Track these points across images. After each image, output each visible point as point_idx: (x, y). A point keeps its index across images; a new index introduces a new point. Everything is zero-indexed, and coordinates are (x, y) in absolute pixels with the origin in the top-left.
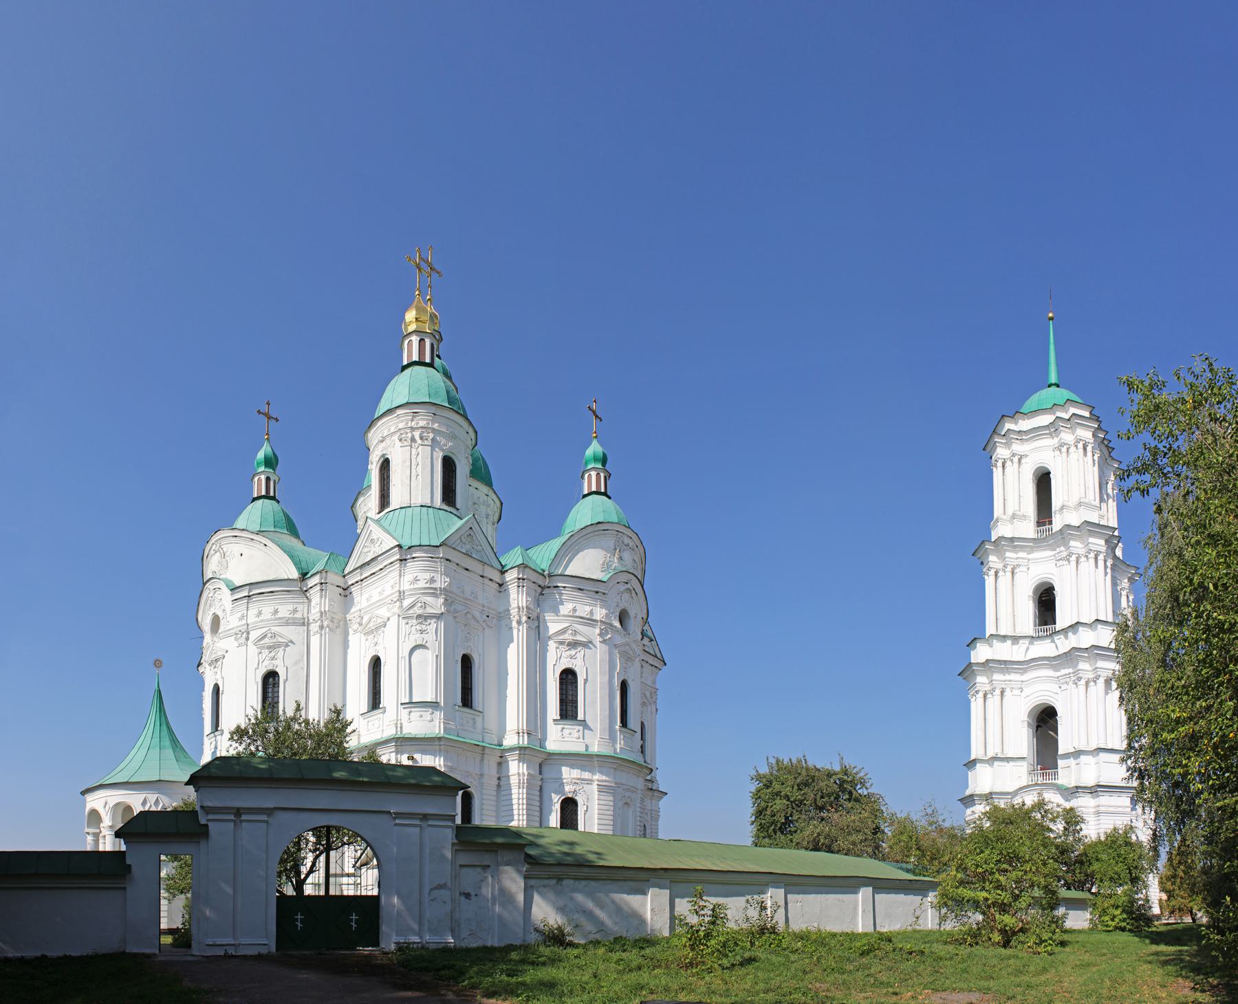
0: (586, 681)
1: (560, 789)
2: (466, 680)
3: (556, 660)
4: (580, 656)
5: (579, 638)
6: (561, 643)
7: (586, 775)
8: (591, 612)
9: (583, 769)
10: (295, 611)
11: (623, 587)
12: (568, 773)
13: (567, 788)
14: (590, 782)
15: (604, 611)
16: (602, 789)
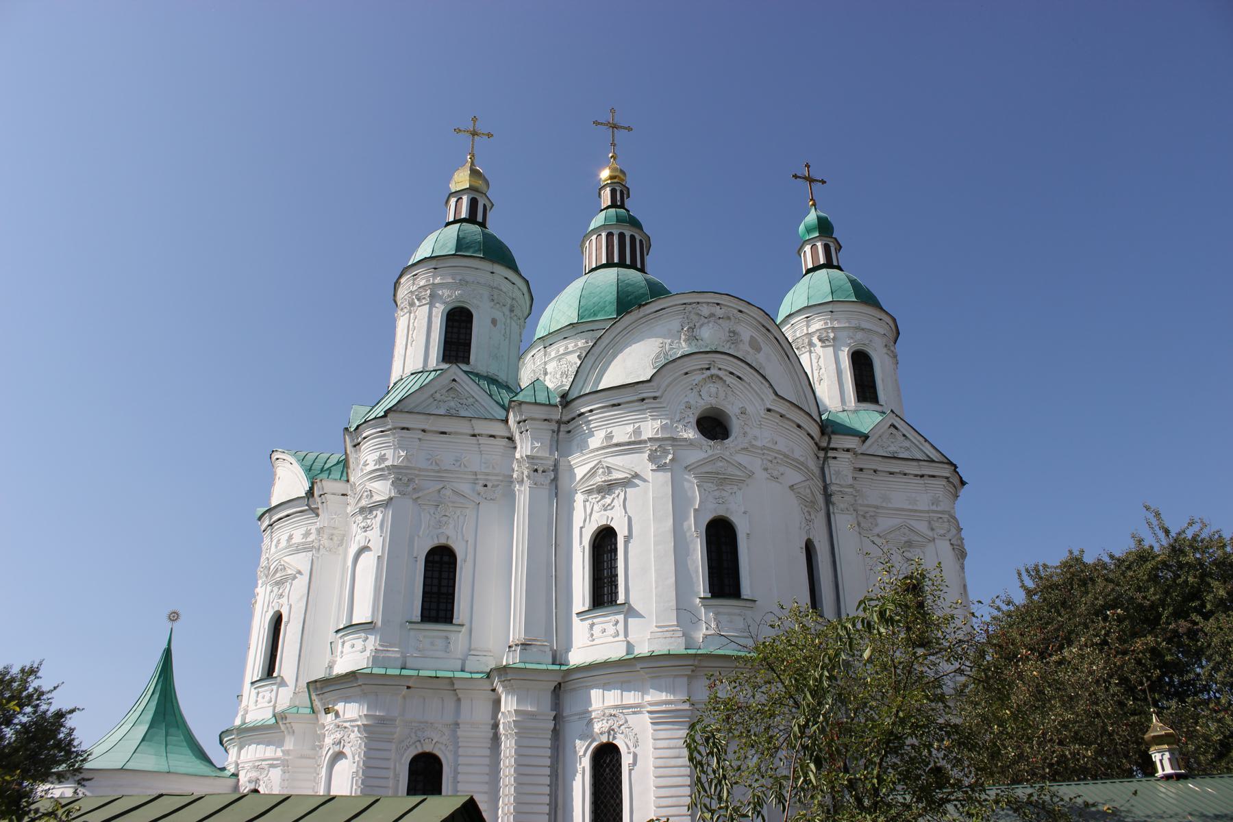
0: (628, 539)
1: (587, 735)
2: (438, 586)
3: (586, 518)
4: (618, 503)
5: (616, 475)
6: (589, 492)
7: (631, 698)
8: (637, 432)
9: (625, 686)
10: (307, 534)
11: (698, 377)
12: (601, 700)
13: (597, 728)
14: (636, 709)
15: (657, 424)
16: (661, 718)
